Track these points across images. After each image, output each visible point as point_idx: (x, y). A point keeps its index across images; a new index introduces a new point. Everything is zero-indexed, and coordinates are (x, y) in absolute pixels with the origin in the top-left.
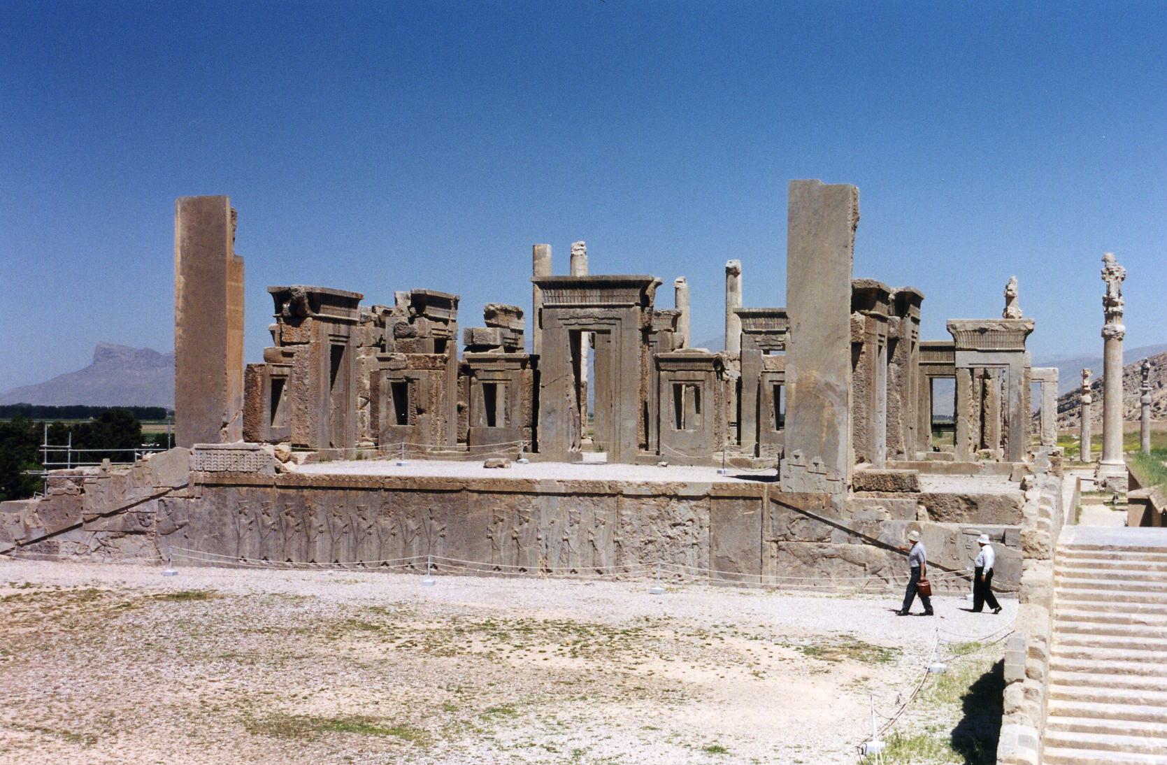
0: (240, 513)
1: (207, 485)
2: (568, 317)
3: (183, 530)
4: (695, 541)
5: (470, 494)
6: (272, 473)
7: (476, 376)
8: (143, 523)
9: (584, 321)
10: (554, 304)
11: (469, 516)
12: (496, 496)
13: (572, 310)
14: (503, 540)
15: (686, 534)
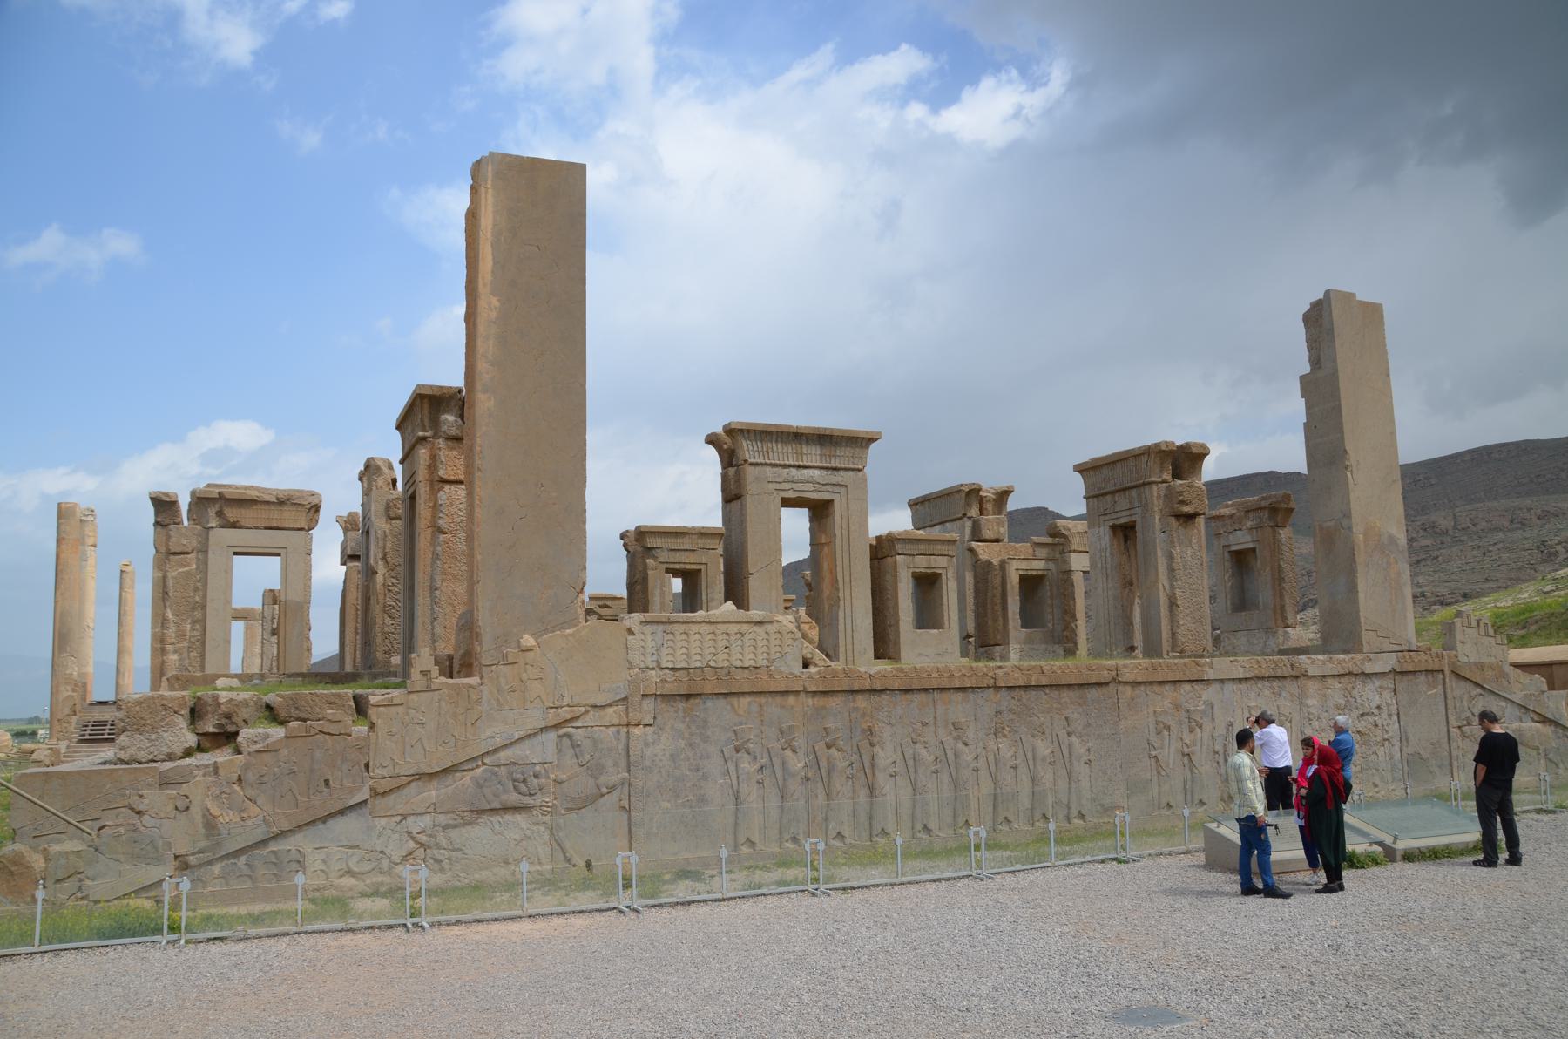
0: (737, 751)
1: (667, 697)
2: (781, 480)
3: (615, 794)
4: (1386, 736)
5: (1121, 688)
6: (797, 668)
7: (655, 558)
8: (523, 788)
9: (801, 486)
10: (763, 461)
11: (1123, 724)
12: (1156, 688)
13: (786, 470)
14: (1171, 762)
15: (1376, 726)
